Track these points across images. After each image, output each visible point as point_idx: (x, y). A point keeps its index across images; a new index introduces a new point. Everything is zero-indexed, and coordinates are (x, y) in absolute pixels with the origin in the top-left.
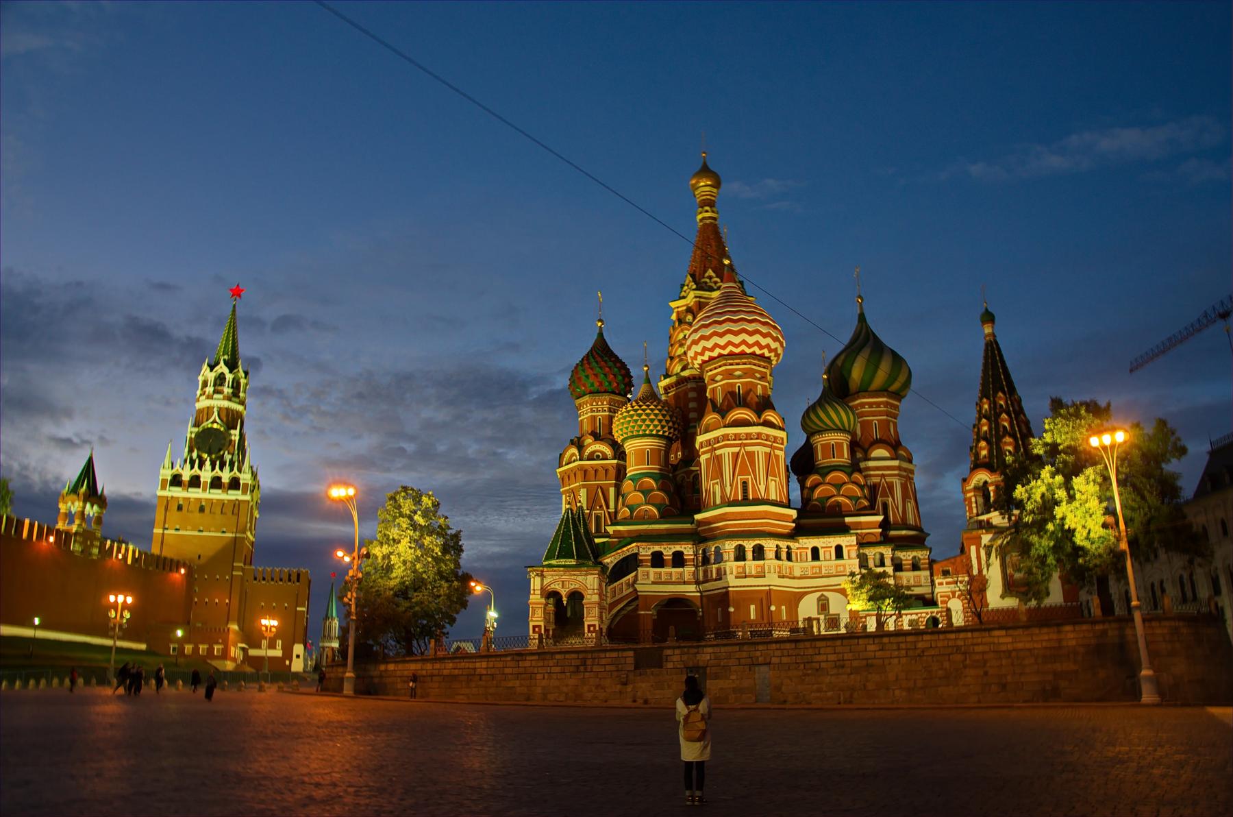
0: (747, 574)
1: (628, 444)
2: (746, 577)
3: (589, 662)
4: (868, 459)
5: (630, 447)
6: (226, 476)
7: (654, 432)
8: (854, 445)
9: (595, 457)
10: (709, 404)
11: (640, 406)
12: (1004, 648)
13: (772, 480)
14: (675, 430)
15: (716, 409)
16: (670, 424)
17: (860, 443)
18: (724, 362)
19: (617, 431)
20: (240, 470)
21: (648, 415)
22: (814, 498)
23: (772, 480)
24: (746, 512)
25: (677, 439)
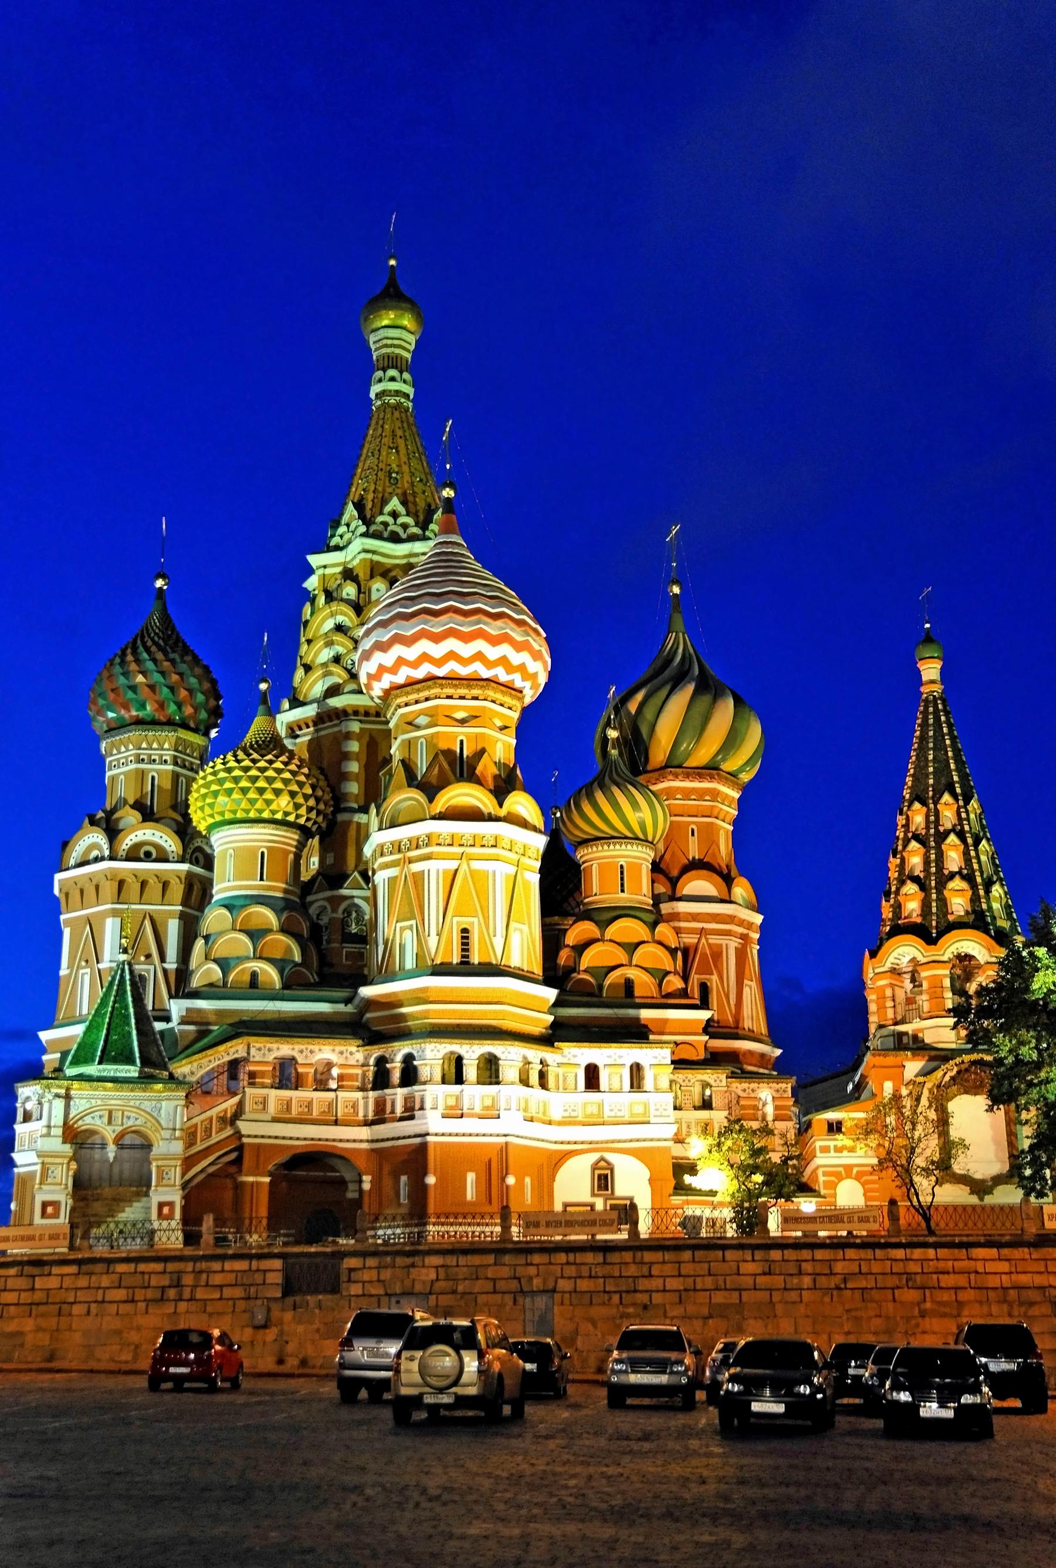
0: (465, 1111)
1: (221, 834)
7: (279, 816)
11: (254, 761)
14: (318, 813)
16: (312, 802)
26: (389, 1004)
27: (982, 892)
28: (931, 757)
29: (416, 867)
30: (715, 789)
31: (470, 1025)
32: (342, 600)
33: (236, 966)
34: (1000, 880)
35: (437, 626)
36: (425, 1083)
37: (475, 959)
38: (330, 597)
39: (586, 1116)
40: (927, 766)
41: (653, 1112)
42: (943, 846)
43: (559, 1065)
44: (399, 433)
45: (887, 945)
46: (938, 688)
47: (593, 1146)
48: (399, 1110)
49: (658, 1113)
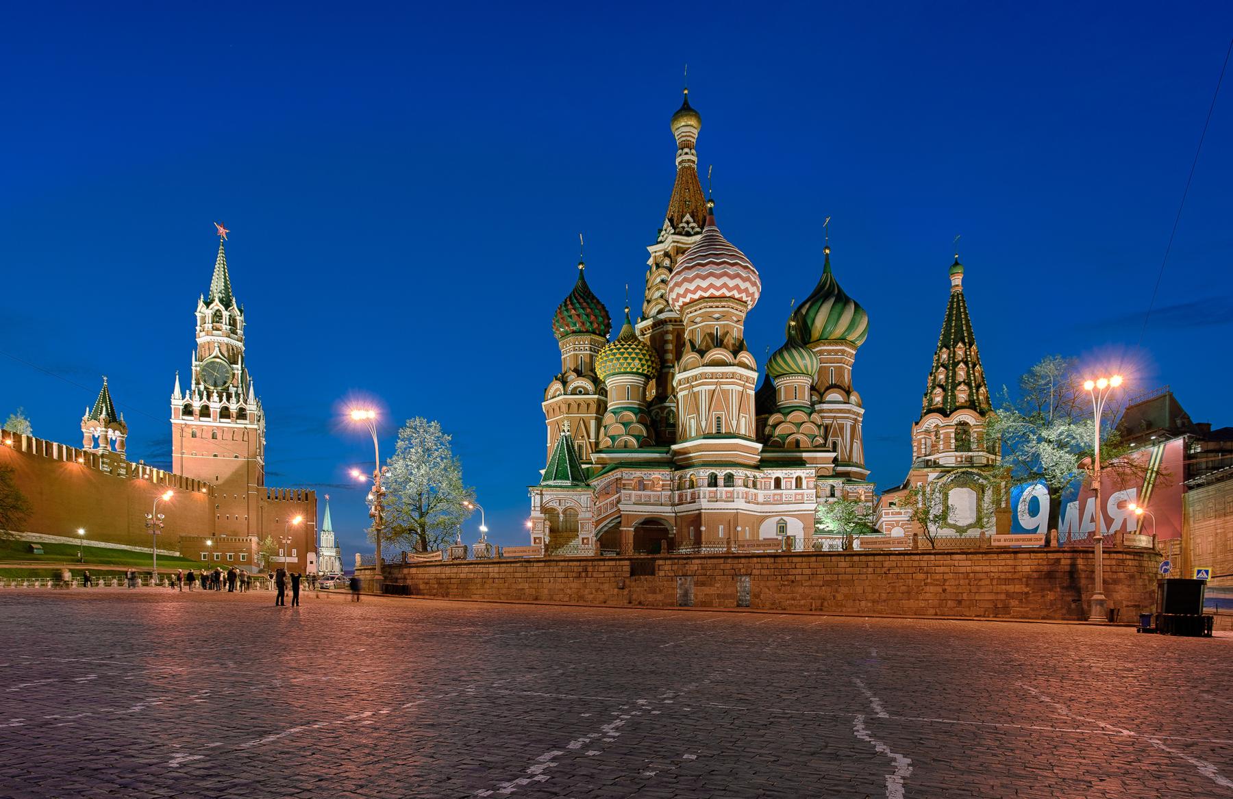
5: (610, 383)
6: (233, 407)
7: (634, 370)
8: (813, 388)
10: (688, 345)
11: (623, 345)
14: (653, 368)
16: (649, 363)
17: (817, 388)
20: (245, 402)
21: (629, 354)
23: (743, 417)
25: (654, 376)
26: (684, 452)
27: (974, 391)
32: (664, 267)
34: (985, 385)
36: (700, 487)
38: (658, 266)
40: (951, 329)
41: (806, 498)
42: (956, 369)
43: (762, 478)
44: (690, 181)
45: (924, 418)
47: (778, 513)
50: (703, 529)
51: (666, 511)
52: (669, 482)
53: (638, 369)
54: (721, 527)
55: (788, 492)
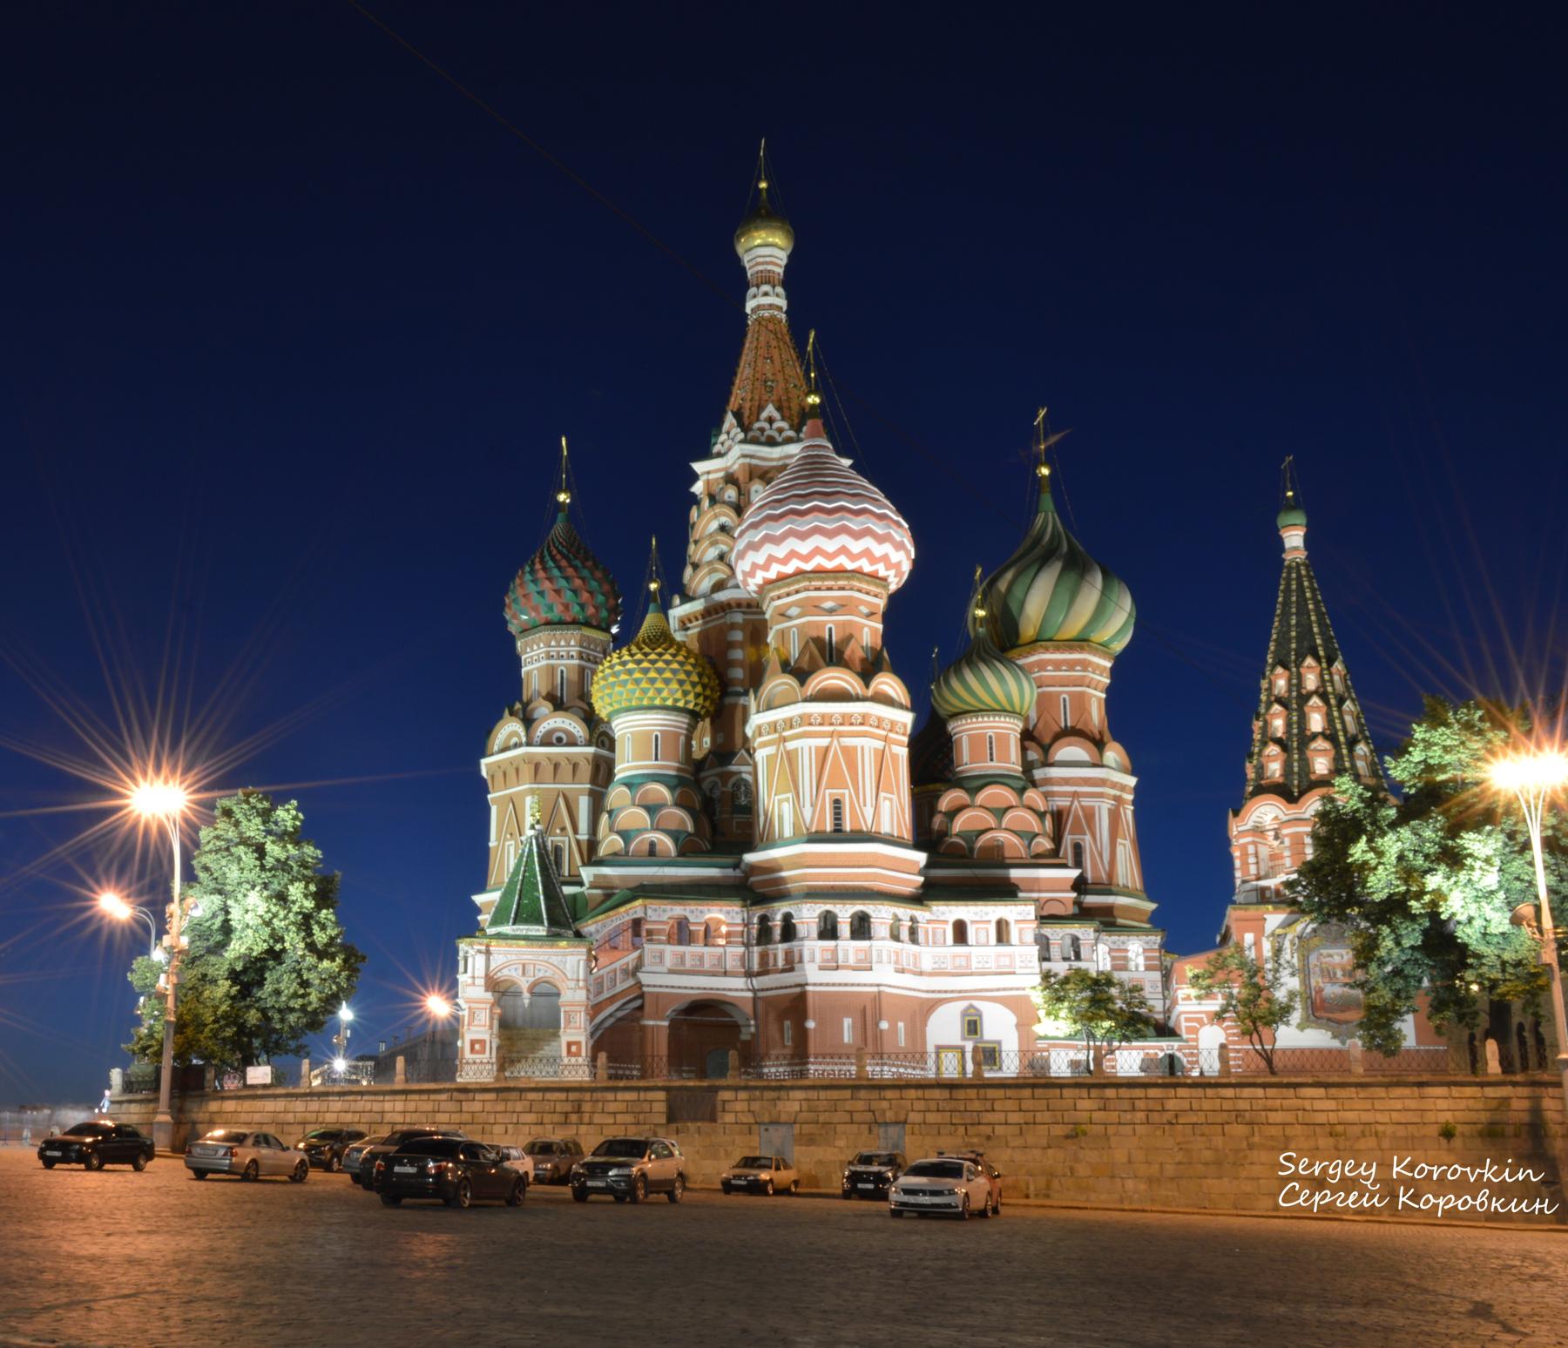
0: (840, 963)
2: (837, 968)
3: (587, 1107)
4: (1047, 763)
5: (625, 727)
7: (669, 703)
8: (1027, 736)
9: (554, 741)
11: (646, 655)
12: (1321, 1118)
13: (885, 798)
14: (706, 698)
15: (786, 667)
16: (699, 689)
18: (806, 583)
19: (602, 698)
21: (660, 671)
22: (954, 832)
23: (885, 798)
24: (840, 853)
26: (771, 868)
28: (1293, 622)
29: (791, 745)
30: (1085, 660)
31: (845, 887)
33: (636, 837)
34: (1366, 738)
35: (804, 525)
36: (802, 939)
37: (848, 827)
39: (956, 968)
40: (1289, 631)
41: (1018, 964)
42: (1306, 709)
43: (929, 922)
45: (1249, 804)
46: (1301, 556)
47: (961, 995)
48: (781, 963)
49: (1023, 965)
50: (811, 1024)
51: (735, 987)
52: (740, 929)
53: (676, 700)
54: (847, 1022)
55: (981, 949)
